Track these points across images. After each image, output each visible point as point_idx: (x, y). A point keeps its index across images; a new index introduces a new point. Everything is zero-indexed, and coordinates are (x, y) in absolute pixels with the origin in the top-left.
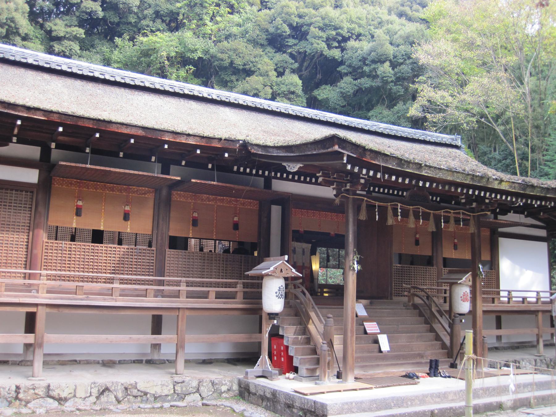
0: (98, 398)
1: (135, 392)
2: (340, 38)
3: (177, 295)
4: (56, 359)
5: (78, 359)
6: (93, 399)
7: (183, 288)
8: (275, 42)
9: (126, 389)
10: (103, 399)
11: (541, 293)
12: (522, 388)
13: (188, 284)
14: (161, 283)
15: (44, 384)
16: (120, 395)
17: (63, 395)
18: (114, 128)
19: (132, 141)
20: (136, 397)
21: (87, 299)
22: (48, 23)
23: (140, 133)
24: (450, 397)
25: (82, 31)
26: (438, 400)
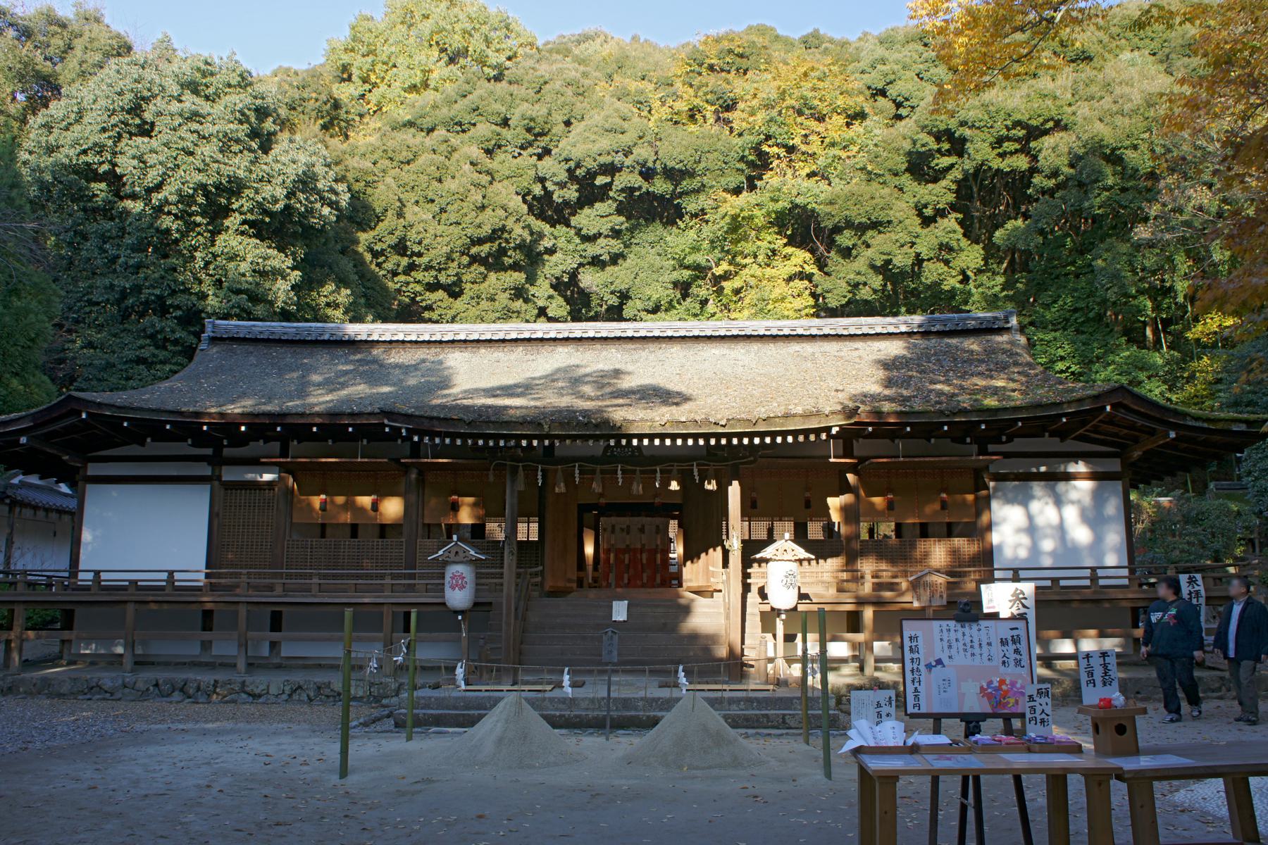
0: (290, 695)
1: (327, 691)
2: (1021, 133)
3: (381, 588)
4: (301, 662)
5: (323, 662)
6: (285, 697)
7: (388, 581)
8: (920, 167)
9: (319, 688)
10: (295, 697)
11: (1020, 572)
12: (726, 703)
13: (394, 577)
14: (412, 576)
15: (240, 680)
16: (312, 694)
17: (257, 691)
18: (289, 420)
19: (315, 429)
20: (328, 697)
21: (286, 596)
22: (574, 221)
23: (318, 420)
24: (584, 705)
25: (622, 219)
26: (561, 706)
